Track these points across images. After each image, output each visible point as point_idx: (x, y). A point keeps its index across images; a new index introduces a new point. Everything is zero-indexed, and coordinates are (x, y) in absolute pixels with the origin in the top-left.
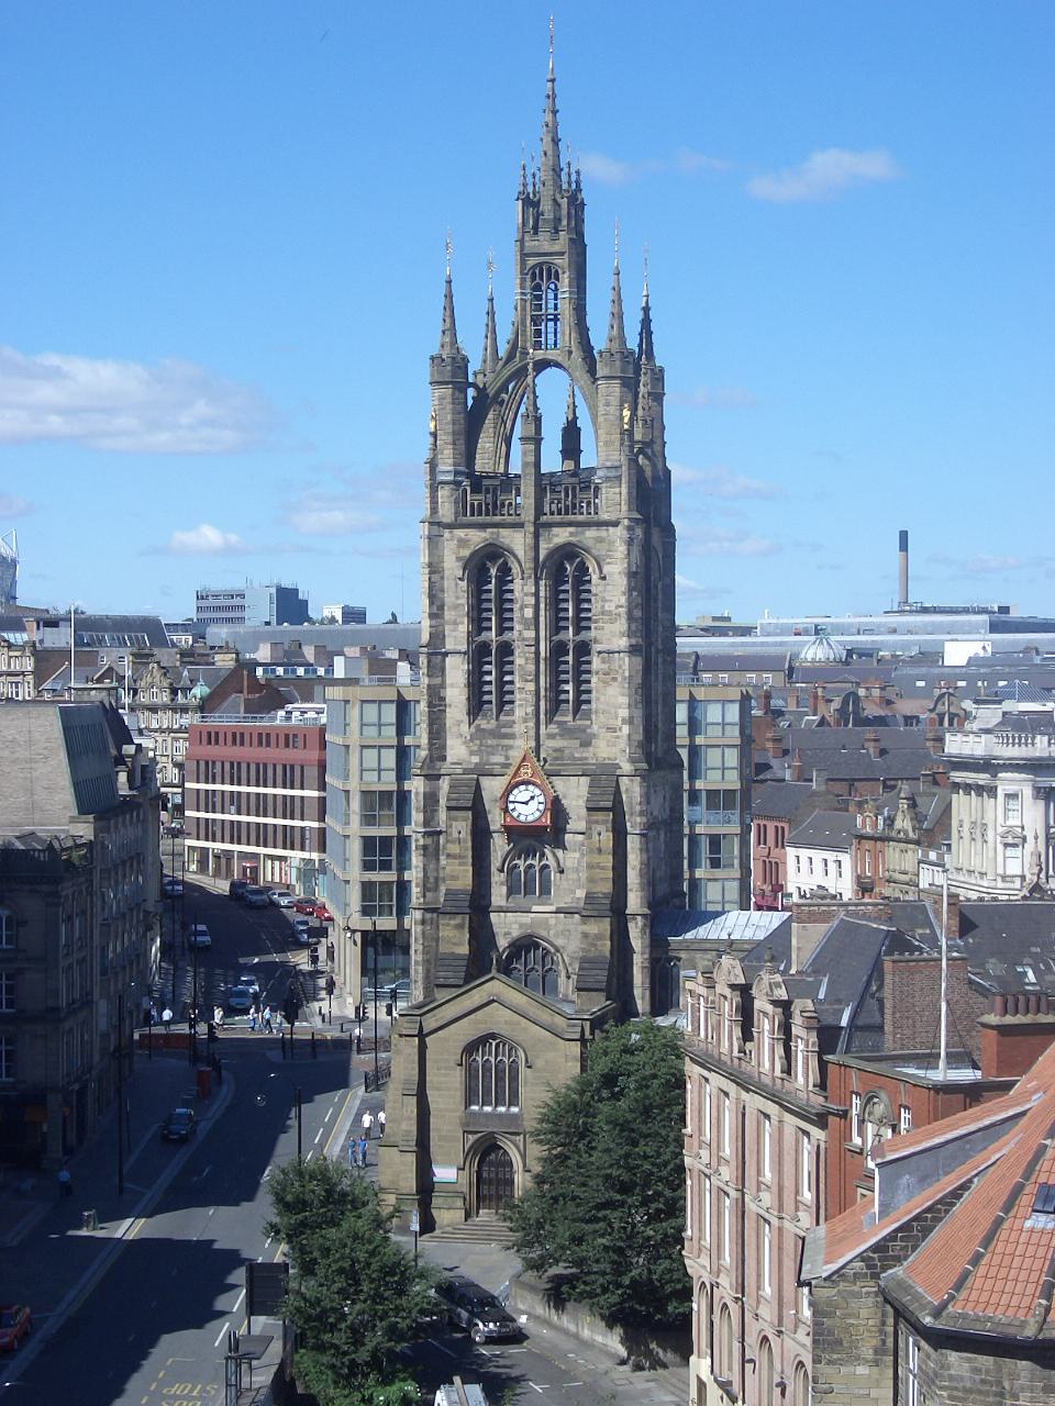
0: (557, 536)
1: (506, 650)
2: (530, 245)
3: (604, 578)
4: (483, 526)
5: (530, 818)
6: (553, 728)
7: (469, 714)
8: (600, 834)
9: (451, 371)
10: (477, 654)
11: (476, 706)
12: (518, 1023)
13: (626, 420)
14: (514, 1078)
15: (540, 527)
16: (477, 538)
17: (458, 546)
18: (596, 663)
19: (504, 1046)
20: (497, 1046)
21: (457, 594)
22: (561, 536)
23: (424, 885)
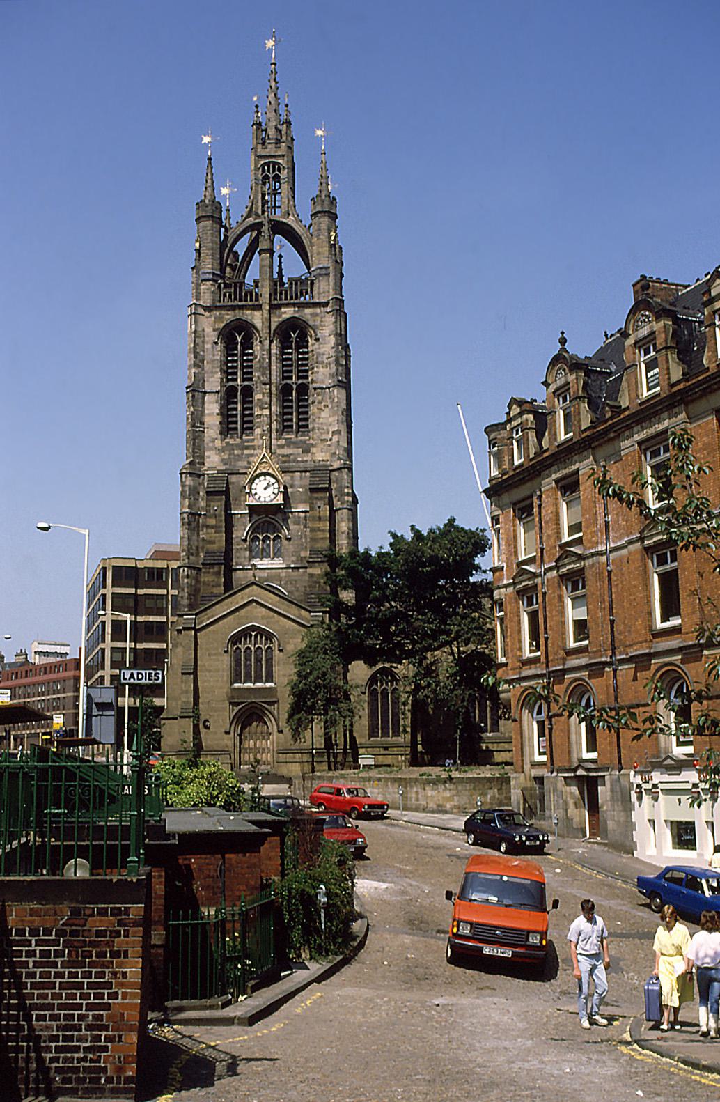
0: (285, 313)
1: (248, 392)
2: (260, 151)
3: (317, 340)
4: (233, 308)
5: (268, 499)
6: (283, 442)
7: (221, 433)
8: (319, 507)
9: (211, 212)
10: (229, 395)
11: (227, 428)
12: (274, 617)
13: (333, 238)
14: (269, 661)
15: (274, 307)
16: (229, 316)
17: (210, 327)
18: (314, 396)
19: (261, 638)
20: (256, 636)
21: (214, 353)
22: (288, 313)
23: (189, 550)
